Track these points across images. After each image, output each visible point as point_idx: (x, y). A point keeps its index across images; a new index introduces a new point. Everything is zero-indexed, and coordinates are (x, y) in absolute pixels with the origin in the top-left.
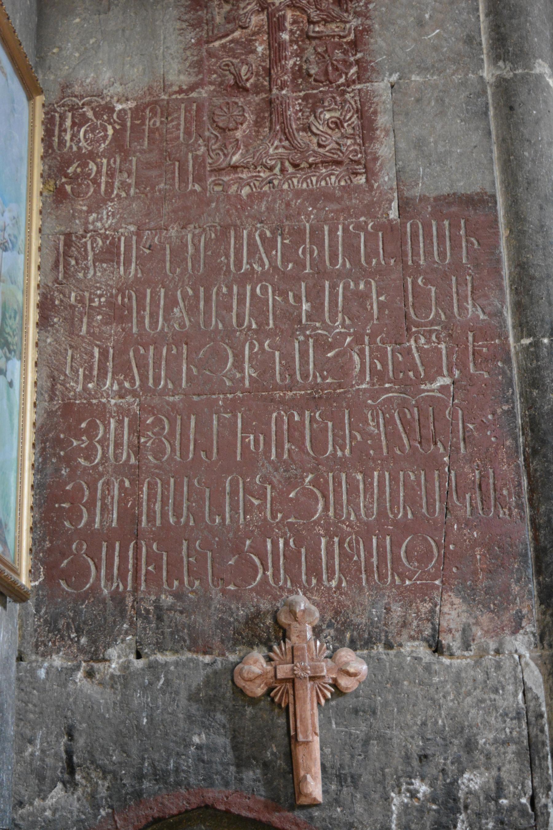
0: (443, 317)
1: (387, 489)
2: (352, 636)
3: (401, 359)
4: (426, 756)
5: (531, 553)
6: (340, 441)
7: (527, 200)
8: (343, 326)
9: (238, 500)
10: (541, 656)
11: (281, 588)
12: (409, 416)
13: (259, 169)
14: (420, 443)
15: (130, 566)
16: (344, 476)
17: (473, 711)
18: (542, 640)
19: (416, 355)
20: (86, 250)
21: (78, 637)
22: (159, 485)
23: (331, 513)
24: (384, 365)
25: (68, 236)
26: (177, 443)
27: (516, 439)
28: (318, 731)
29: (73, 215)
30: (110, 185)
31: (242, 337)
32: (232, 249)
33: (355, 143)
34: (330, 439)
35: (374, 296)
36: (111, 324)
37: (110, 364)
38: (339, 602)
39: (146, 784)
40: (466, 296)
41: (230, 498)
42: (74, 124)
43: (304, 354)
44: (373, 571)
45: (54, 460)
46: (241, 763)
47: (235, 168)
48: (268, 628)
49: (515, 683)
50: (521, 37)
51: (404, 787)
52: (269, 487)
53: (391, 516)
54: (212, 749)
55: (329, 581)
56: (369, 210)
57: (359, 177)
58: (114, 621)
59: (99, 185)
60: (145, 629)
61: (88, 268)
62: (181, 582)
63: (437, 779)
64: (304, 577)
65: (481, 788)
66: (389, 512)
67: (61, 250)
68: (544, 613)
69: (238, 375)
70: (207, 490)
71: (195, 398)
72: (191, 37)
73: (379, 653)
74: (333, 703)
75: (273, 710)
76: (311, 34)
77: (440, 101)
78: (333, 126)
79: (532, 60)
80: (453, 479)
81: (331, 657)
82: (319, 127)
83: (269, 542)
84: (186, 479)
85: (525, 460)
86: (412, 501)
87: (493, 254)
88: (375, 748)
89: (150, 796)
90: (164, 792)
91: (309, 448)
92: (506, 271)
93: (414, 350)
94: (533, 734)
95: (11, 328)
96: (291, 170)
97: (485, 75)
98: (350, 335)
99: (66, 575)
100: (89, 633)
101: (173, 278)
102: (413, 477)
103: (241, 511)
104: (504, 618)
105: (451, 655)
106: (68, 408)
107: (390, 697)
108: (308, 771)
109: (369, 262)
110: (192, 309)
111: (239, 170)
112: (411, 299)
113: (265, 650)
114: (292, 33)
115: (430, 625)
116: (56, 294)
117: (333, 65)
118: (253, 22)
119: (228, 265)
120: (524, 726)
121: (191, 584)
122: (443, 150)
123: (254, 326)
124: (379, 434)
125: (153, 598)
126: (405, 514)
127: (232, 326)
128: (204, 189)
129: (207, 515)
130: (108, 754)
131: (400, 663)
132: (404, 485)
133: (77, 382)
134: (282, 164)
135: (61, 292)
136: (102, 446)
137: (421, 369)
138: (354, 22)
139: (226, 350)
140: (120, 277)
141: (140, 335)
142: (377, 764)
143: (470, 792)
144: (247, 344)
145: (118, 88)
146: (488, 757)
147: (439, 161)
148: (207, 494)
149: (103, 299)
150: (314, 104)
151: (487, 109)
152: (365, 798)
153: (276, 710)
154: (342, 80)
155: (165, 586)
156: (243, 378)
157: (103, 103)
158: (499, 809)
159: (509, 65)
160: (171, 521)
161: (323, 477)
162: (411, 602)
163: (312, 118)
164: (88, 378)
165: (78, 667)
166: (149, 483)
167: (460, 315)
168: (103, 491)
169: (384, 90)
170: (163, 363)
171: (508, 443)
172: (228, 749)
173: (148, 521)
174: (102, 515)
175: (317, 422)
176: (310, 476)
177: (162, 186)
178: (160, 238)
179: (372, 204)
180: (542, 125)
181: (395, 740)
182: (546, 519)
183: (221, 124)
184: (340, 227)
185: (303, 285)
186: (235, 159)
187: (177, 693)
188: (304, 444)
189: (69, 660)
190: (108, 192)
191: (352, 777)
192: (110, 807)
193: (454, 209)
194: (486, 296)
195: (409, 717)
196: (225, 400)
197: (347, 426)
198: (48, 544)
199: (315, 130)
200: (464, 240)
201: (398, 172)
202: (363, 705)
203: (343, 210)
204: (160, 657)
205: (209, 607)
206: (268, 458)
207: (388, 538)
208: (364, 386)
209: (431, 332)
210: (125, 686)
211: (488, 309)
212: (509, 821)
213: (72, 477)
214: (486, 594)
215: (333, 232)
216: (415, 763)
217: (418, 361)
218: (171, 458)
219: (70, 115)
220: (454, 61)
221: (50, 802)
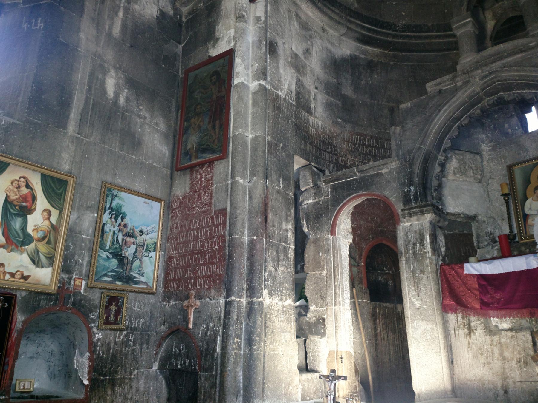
47: (194, 208)
138: (212, 174)
150: (205, 192)
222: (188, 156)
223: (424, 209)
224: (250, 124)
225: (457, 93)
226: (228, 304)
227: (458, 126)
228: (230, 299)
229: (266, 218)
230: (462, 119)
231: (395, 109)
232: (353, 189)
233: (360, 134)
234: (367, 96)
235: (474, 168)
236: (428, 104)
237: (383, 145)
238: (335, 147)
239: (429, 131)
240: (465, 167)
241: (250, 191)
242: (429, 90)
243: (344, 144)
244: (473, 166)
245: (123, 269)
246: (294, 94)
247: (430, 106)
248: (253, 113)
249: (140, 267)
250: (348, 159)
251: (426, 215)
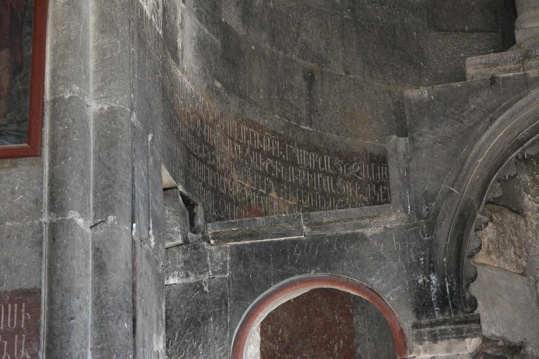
7: (56, 291)
50: (62, 199)
77: (19, 236)
79: (67, 212)
87: (37, 322)
159: (55, 215)
193: (20, 298)
194: (31, 345)
200: (23, 314)
211: (32, 352)
223: (465, 327)
224: (91, 76)
225: (529, 92)
227: (517, 157)
229: (134, 320)
230: (526, 145)
231: (316, 77)
232: (292, 264)
233: (253, 125)
234: (264, 35)
235: (517, 244)
236: (467, 102)
237: (295, 157)
238: (212, 148)
239: (469, 160)
240: (504, 240)
241: (97, 250)
242: (470, 71)
243: (226, 143)
244: (515, 239)
246: (160, 10)
247: (473, 107)
248: (101, 52)
250: (233, 180)
251: (467, 340)
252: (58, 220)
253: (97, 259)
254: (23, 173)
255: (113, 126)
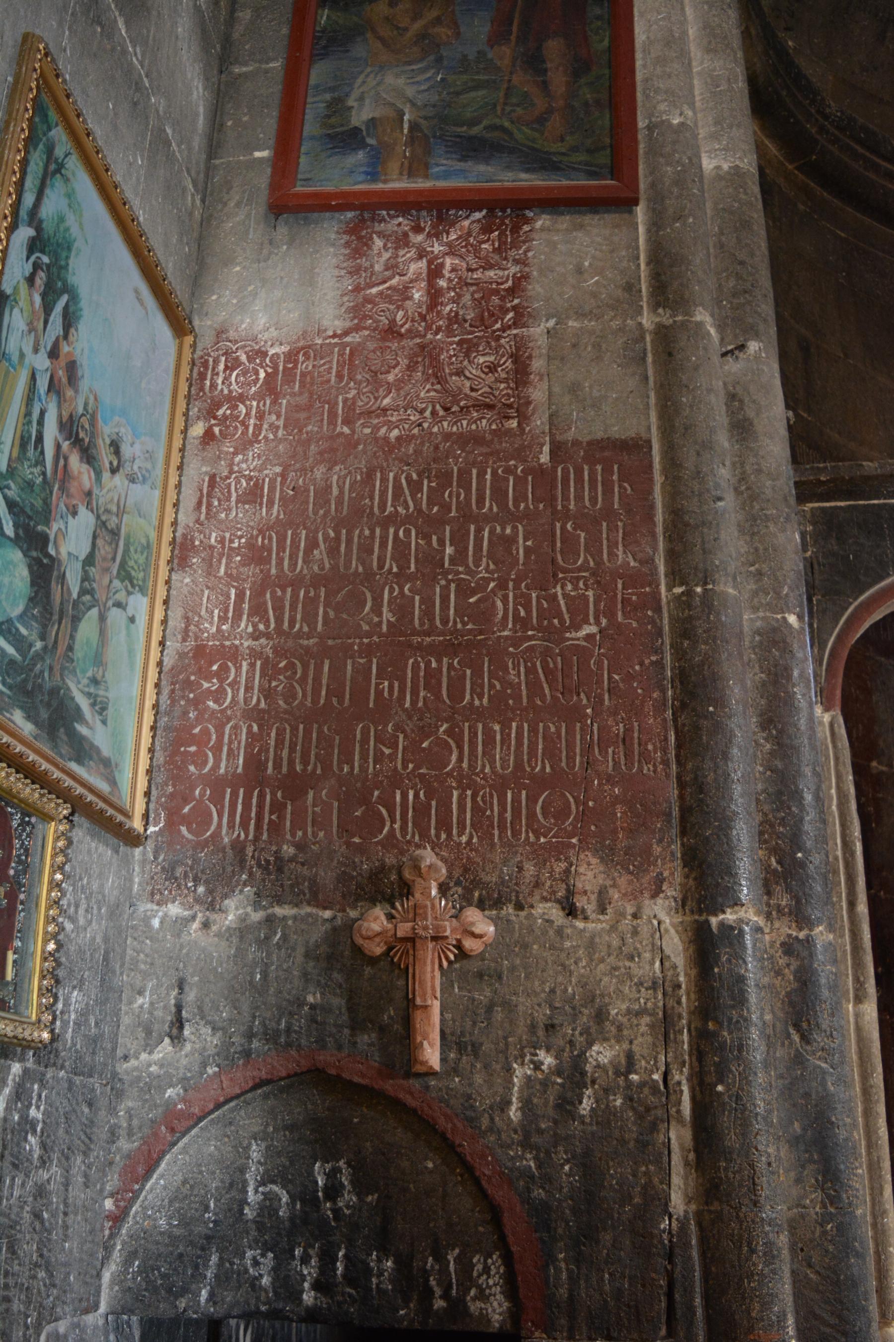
0: (592, 564)
1: (526, 741)
2: (480, 895)
3: (545, 606)
4: (553, 1026)
5: (676, 812)
6: (478, 690)
7: (684, 446)
8: (487, 571)
9: (368, 749)
10: (682, 923)
11: (409, 842)
12: (551, 665)
13: (409, 412)
14: (562, 693)
15: (253, 815)
16: (480, 726)
17: (606, 979)
18: (684, 905)
19: (562, 602)
20: (229, 492)
21: (195, 886)
22: (288, 731)
23: (465, 765)
24: (528, 611)
25: (213, 478)
26: (309, 688)
27: (663, 691)
28: (438, 995)
29: (219, 457)
30: (258, 428)
31: (383, 580)
32: (377, 492)
33: (508, 387)
34: (468, 687)
35: (521, 542)
36: (249, 565)
37: (246, 606)
38: (468, 858)
39: (255, 1044)
40: (617, 543)
41: (361, 746)
42: (226, 368)
43: (445, 599)
44: (506, 828)
45: (182, 703)
46: (356, 1026)
47: (385, 410)
48: (393, 883)
49: (653, 950)
50: (681, 284)
51: (528, 1058)
52: (401, 736)
53: (528, 769)
54: (326, 1009)
55: (459, 836)
56: (519, 454)
57: (511, 421)
58: (233, 871)
59: (247, 427)
60: (264, 880)
61: (230, 510)
62: (305, 833)
63: (563, 1051)
64: (433, 832)
65: (611, 1062)
66: (526, 765)
67: (205, 491)
68: (687, 877)
69: (376, 619)
70: (337, 737)
71: (330, 642)
72: (348, 284)
73: (509, 914)
74: (457, 966)
75: (393, 971)
76: (469, 281)
77: (597, 346)
78: (486, 370)
80: (596, 732)
81: (456, 917)
82: (472, 371)
83: (398, 792)
84: (315, 726)
85: (673, 714)
86: (551, 753)
88: (499, 1015)
89: (258, 1056)
90: (274, 1053)
91: (445, 696)
92: (659, 517)
93: (560, 597)
94: (669, 1006)
95: (136, 562)
96: (441, 413)
97: (644, 322)
98: (493, 580)
99: (186, 821)
100: (207, 882)
101: (315, 520)
102: (553, 729)
103: (371, 760)
104: (643, 881)
105: (586, 918)
106: (200, 651)
107: (518, 962)
108: (425, 1038)
109: (516, 506)
110: (333, 551)
111: (389, 412)
112: (559, 545)
113: (388, 906)
114: (450, 280)
115: (564, 886)
116: (196, 534)
117: (488, 310)
118: (411, 271)
119: (372, 508)
120: (660, 996)
121: (315, 835)
122: (598, 394)
123: (395, 570)
124: (519, 684)
125: (274, 848)
126: (543, 768)
127: (372, 569)
128: (353, 432)
129: (335, 763)
130: (218, 1010)
131: (531, 926)
132: (544, 738)
133: (211, 623)
134: (434, 407)
135: (201, 532)
136: (233, 690)
137: (566, 617)
138: (514, 269)
139: (364, 593)
140: (262, 518)
141: (277, 576)
142: (500, 1032)
143: (598, 1066)
144: (387, 588)
145: (273, 333)
146: (620, 1028)
147: (593, 406)
148: (337, 741)
149: (243, 540)
150: (468, 348)
151: (645, 354)
152: (485, 1067)
153: (397, 971)
154: (498, 326)
155: (288, 837)
156: (381, 622)
157: (257, 347)
158: (629, 1085)
159: (669, 312)
160: (298, 769)
161: (459, 727)
162: (545, 861)
163: (466, 363)
164: (223, 619)
165: (194, 918)
166: (278, 728)
167: (609, 561)
168: (230, 736)
169: (541, 335)
170: (300, 605)
171: (655, 695)
172: (343, 1010)
173: (274, 769)
174: (228, 760)
175: (455, 669)
176: (445, 726)
177: (309, 428)
178: (304, 480)
179: (522, 448)
180: (701, 372)
181: (521, 1008)
182: (692, 776)
183: (373, 368)
184: (489, 471)
185: (448, 528)
186: (386, 401)
187: (294, 949)
188: (440, 691)
189: (185, 909)
190: (256, 435)
191: (473, 1045)
192: (218, 1066)
193: (606, 454)
195: (537, 983)
196: (361, 644)
197: (486, 674)
198: (170, 789)
199: (468, 374)
201: (551, 416)
202: (489, 969)
203: (491, 454)
204: (279, 911)
205: (332, 860)
206: (402, 705)
207: (524, 792)
208: (506, 633)
209: (578, 579)
210: (241, 938)
211: (640, 556)
212: (639, 1098)
213: (199, 720)
214: (626, 854)
215: (481, 475)
216: (541, 1033)
217: (564, 609)
218: (301, 703)
219: (223, 359)
220: (613, 308)
221: (157, 1056)
222: (361, 155)
226: (708, 948)
228: (729, 916)
241: (732, 397)
245: (43, 637)
249: (99, 660)
252: (675, 322)
253: (733, 412)
254: (599, 239)
255: (742, 196)
